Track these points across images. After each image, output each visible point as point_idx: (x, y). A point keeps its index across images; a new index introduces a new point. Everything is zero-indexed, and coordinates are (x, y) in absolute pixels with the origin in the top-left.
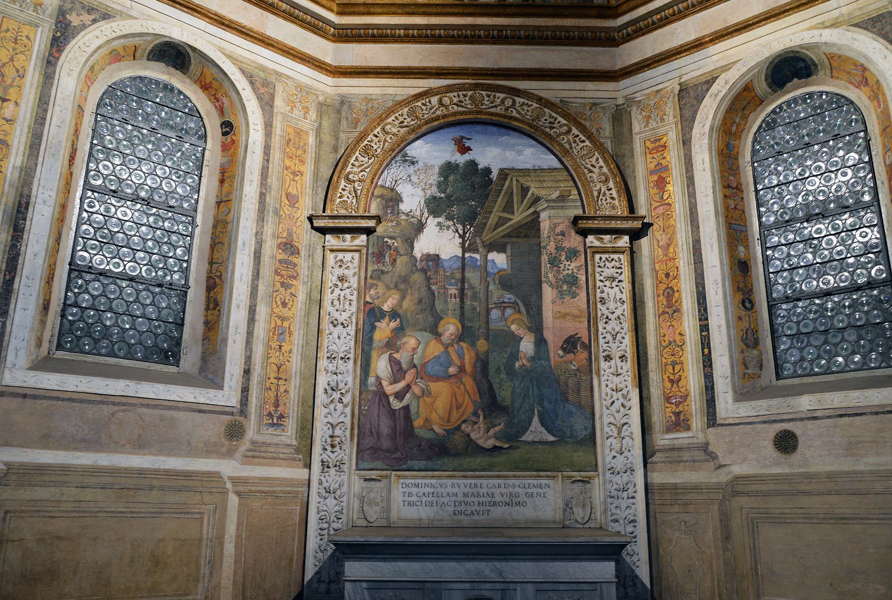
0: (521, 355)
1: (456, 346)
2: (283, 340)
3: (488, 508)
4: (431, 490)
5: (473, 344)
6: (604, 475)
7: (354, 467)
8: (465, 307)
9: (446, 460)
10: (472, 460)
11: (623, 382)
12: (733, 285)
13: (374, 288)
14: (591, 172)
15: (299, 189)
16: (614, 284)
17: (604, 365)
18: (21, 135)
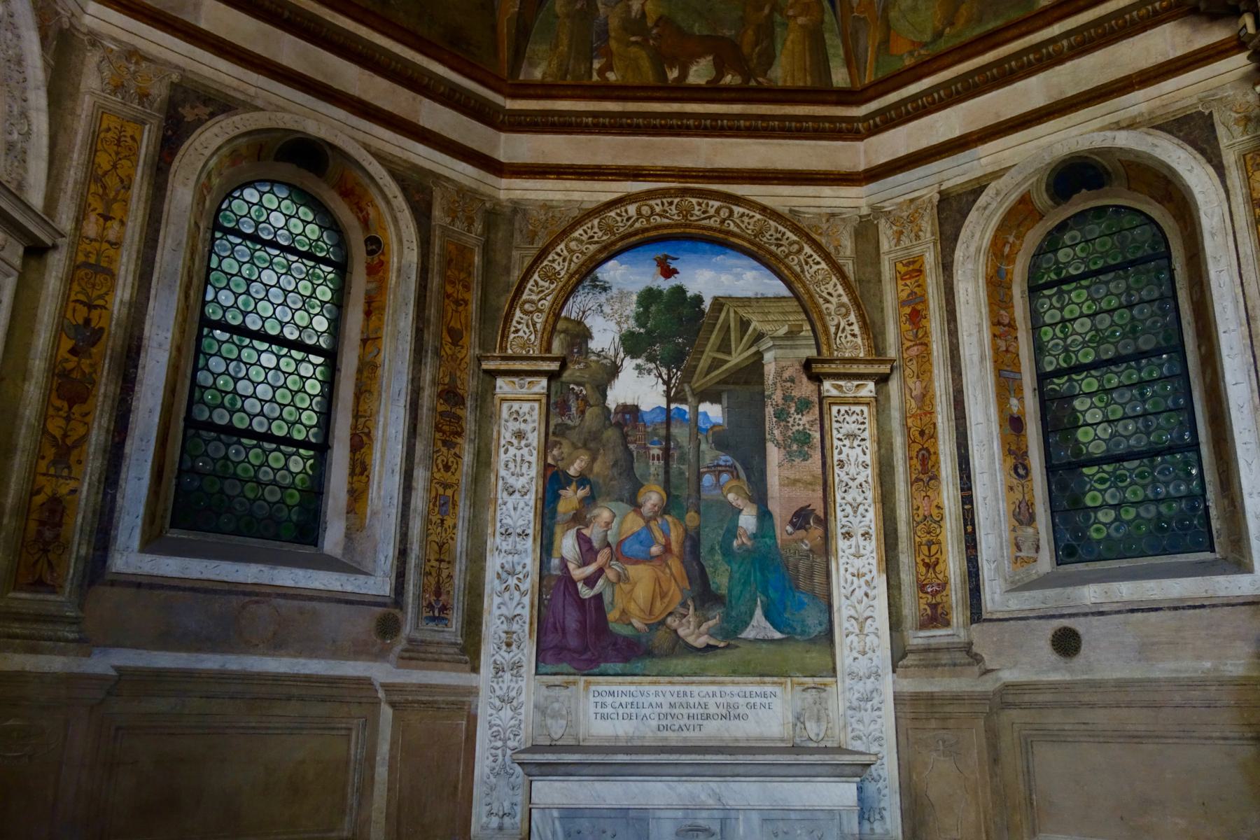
0: (740, 531)
1: (660, 521)
3: (700, 722)
4: (630, 700)
5: (680, 518)
6: (844, 682)
7: (533, 672)
8: (671, 471)
9: (647, 662)
10: (680, 662)
12: (1003, 446)
14: (827, 301)
15: (463, 321)
16: (856, 443)
17: (842, 544)
18: (128, 261)
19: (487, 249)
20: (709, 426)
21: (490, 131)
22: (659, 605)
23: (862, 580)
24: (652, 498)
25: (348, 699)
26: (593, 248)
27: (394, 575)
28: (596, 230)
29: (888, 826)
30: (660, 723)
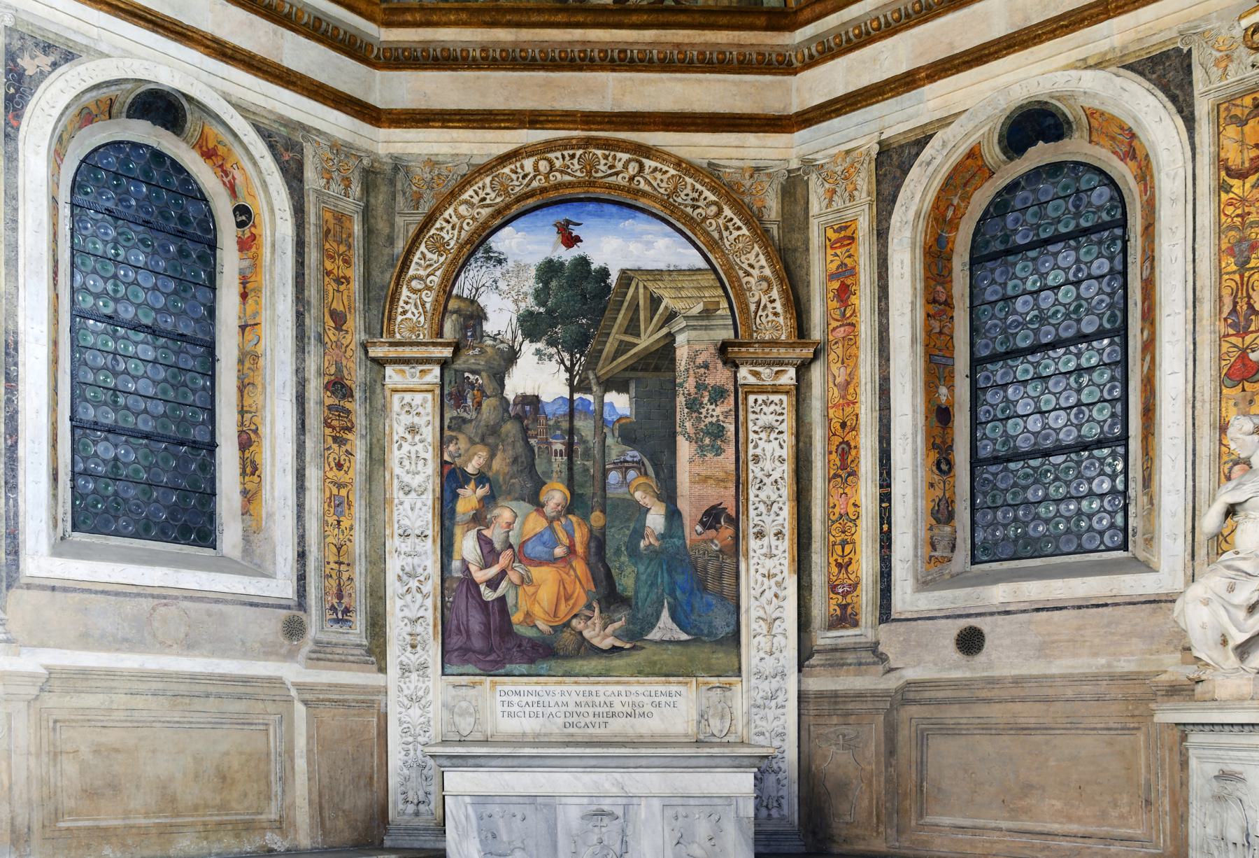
0: (648, 531)
1: (563, 520)
2: (342, 513)
3: (606, 719)
4: (536, 699)
5: (585, 517)
6: (749, 681)
8: (575, 468)
9: (553, 663)
10: (585, 663)
11: (778, 566)
13: (454, 442)
15: (346, 303)
16: (773, 435)
17: (753, 544)
19: (367, 214)
20: (615, 418)
21: (362, 69)
22: (563, 609)
23: (773, 581)
24: (555, 495)
25: (263, 697)
26: (485, 212)
27: (295, 578)
28: (488, 190)
29: (785, 811)
30: (567, 720)
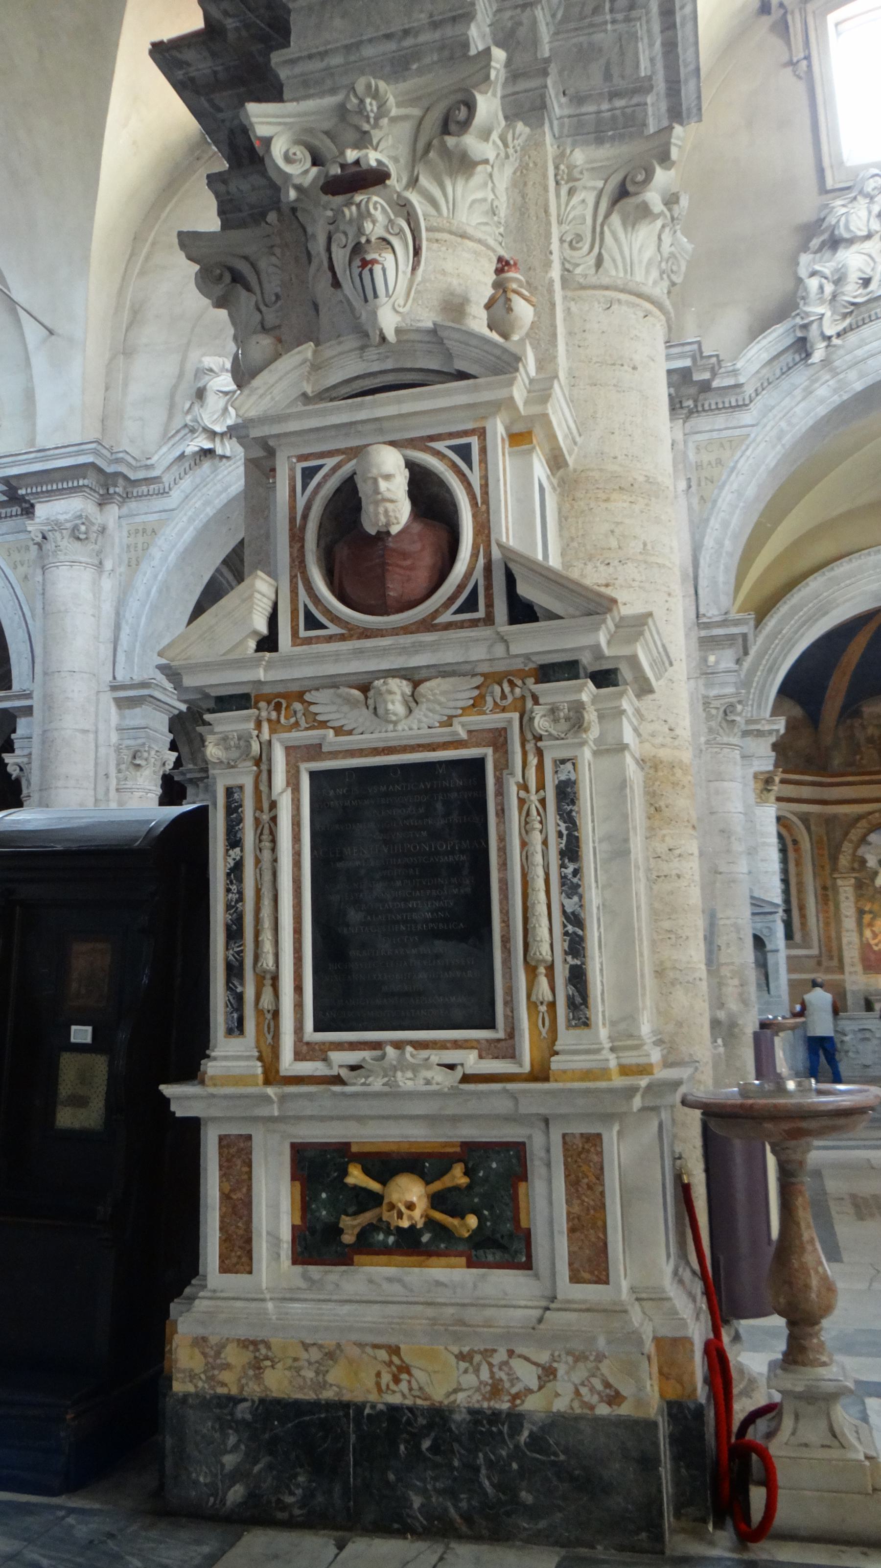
19: (827, 833)
